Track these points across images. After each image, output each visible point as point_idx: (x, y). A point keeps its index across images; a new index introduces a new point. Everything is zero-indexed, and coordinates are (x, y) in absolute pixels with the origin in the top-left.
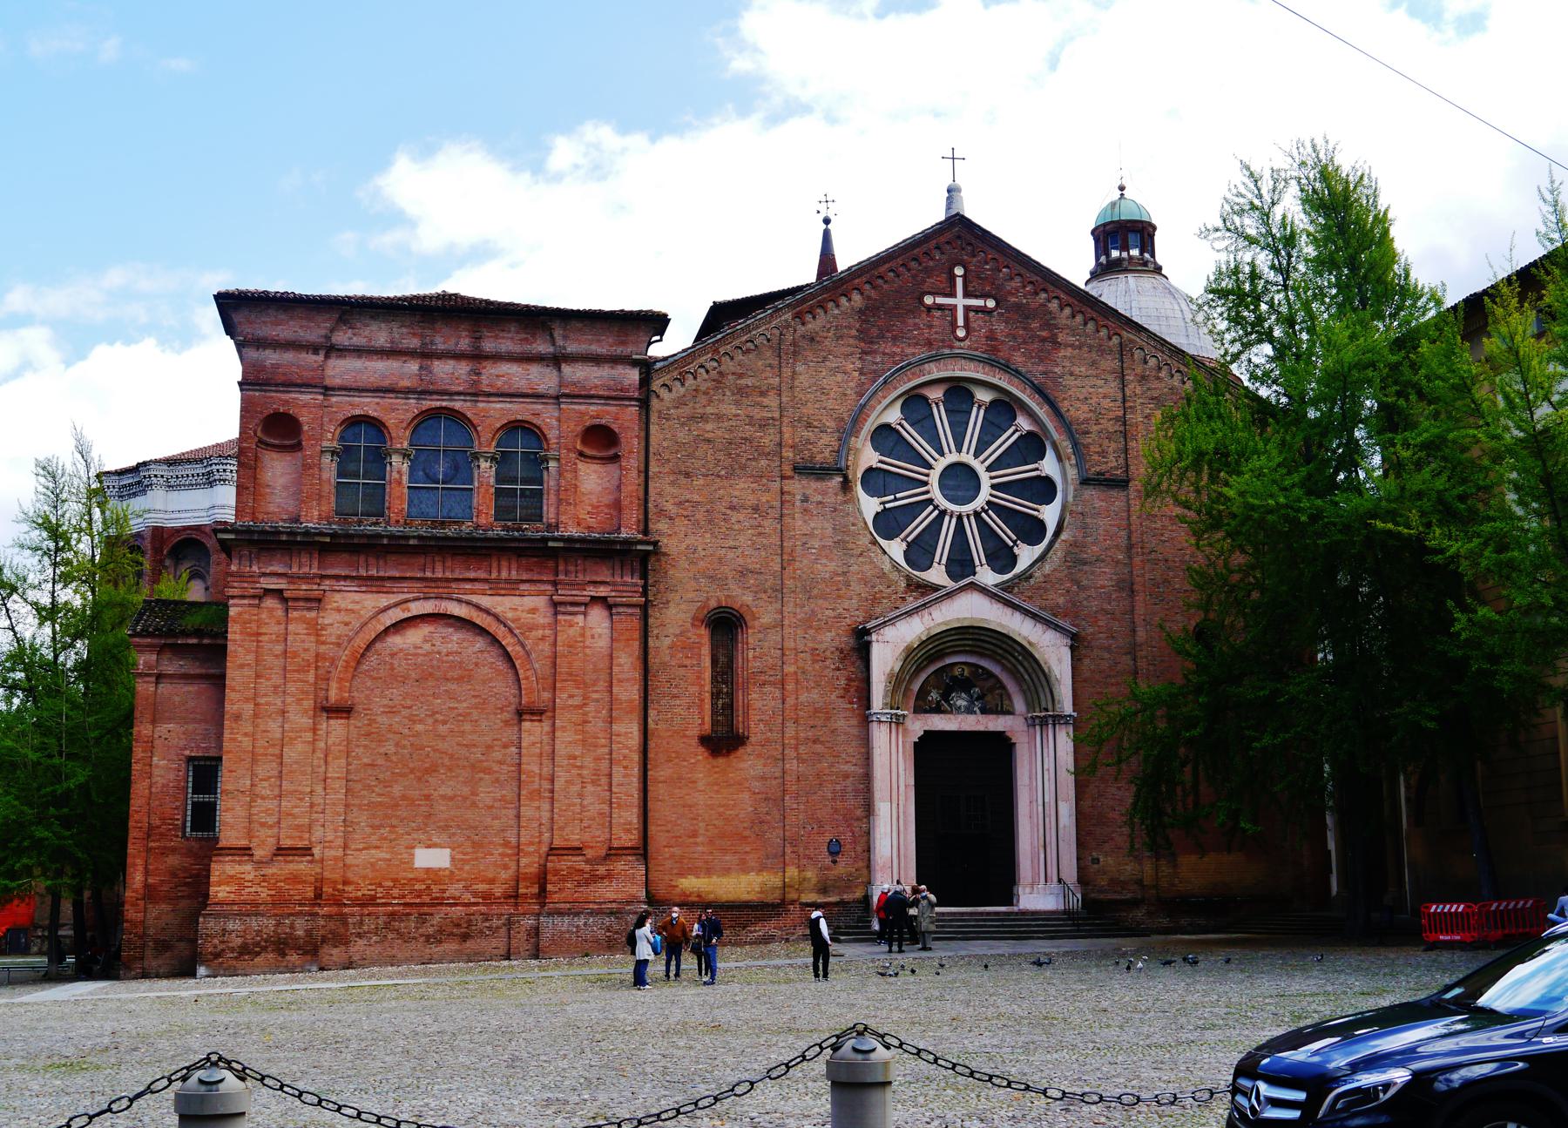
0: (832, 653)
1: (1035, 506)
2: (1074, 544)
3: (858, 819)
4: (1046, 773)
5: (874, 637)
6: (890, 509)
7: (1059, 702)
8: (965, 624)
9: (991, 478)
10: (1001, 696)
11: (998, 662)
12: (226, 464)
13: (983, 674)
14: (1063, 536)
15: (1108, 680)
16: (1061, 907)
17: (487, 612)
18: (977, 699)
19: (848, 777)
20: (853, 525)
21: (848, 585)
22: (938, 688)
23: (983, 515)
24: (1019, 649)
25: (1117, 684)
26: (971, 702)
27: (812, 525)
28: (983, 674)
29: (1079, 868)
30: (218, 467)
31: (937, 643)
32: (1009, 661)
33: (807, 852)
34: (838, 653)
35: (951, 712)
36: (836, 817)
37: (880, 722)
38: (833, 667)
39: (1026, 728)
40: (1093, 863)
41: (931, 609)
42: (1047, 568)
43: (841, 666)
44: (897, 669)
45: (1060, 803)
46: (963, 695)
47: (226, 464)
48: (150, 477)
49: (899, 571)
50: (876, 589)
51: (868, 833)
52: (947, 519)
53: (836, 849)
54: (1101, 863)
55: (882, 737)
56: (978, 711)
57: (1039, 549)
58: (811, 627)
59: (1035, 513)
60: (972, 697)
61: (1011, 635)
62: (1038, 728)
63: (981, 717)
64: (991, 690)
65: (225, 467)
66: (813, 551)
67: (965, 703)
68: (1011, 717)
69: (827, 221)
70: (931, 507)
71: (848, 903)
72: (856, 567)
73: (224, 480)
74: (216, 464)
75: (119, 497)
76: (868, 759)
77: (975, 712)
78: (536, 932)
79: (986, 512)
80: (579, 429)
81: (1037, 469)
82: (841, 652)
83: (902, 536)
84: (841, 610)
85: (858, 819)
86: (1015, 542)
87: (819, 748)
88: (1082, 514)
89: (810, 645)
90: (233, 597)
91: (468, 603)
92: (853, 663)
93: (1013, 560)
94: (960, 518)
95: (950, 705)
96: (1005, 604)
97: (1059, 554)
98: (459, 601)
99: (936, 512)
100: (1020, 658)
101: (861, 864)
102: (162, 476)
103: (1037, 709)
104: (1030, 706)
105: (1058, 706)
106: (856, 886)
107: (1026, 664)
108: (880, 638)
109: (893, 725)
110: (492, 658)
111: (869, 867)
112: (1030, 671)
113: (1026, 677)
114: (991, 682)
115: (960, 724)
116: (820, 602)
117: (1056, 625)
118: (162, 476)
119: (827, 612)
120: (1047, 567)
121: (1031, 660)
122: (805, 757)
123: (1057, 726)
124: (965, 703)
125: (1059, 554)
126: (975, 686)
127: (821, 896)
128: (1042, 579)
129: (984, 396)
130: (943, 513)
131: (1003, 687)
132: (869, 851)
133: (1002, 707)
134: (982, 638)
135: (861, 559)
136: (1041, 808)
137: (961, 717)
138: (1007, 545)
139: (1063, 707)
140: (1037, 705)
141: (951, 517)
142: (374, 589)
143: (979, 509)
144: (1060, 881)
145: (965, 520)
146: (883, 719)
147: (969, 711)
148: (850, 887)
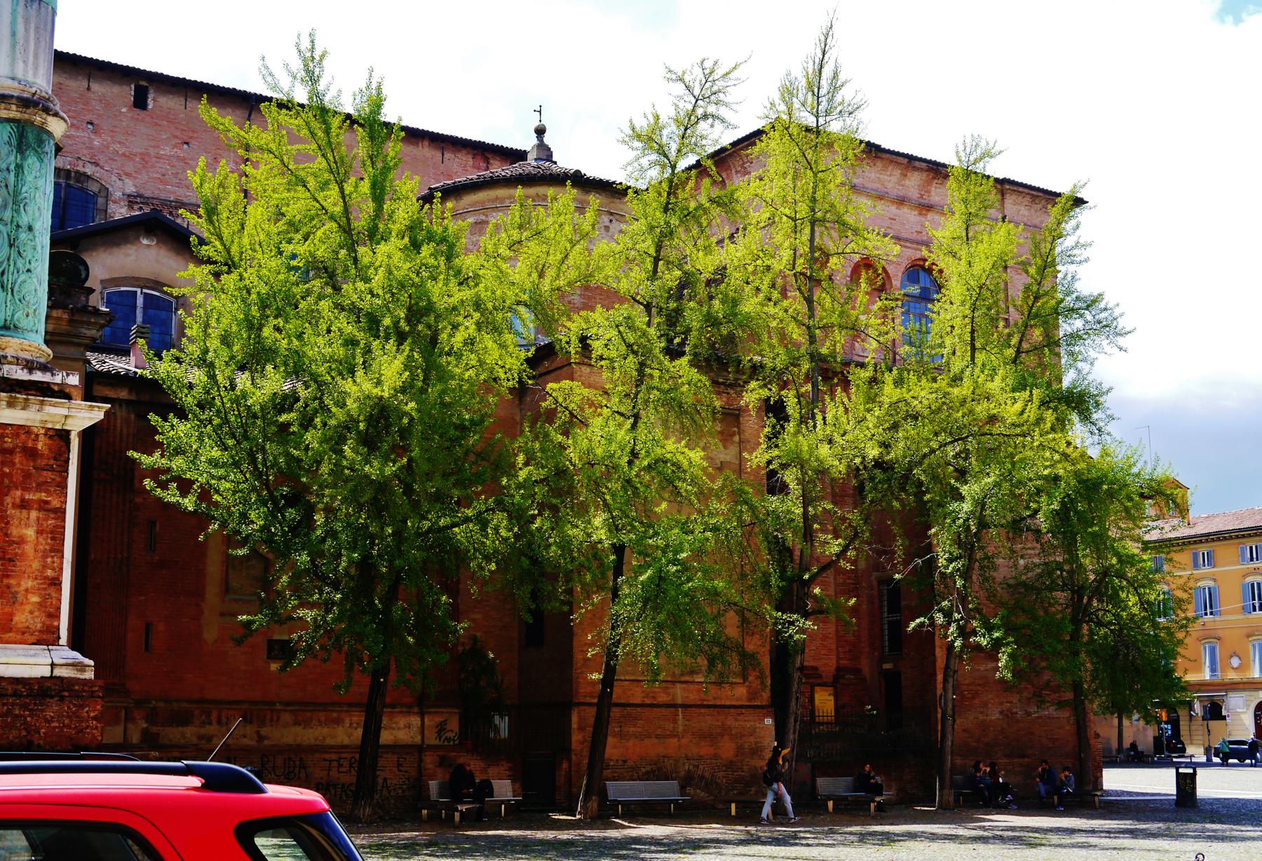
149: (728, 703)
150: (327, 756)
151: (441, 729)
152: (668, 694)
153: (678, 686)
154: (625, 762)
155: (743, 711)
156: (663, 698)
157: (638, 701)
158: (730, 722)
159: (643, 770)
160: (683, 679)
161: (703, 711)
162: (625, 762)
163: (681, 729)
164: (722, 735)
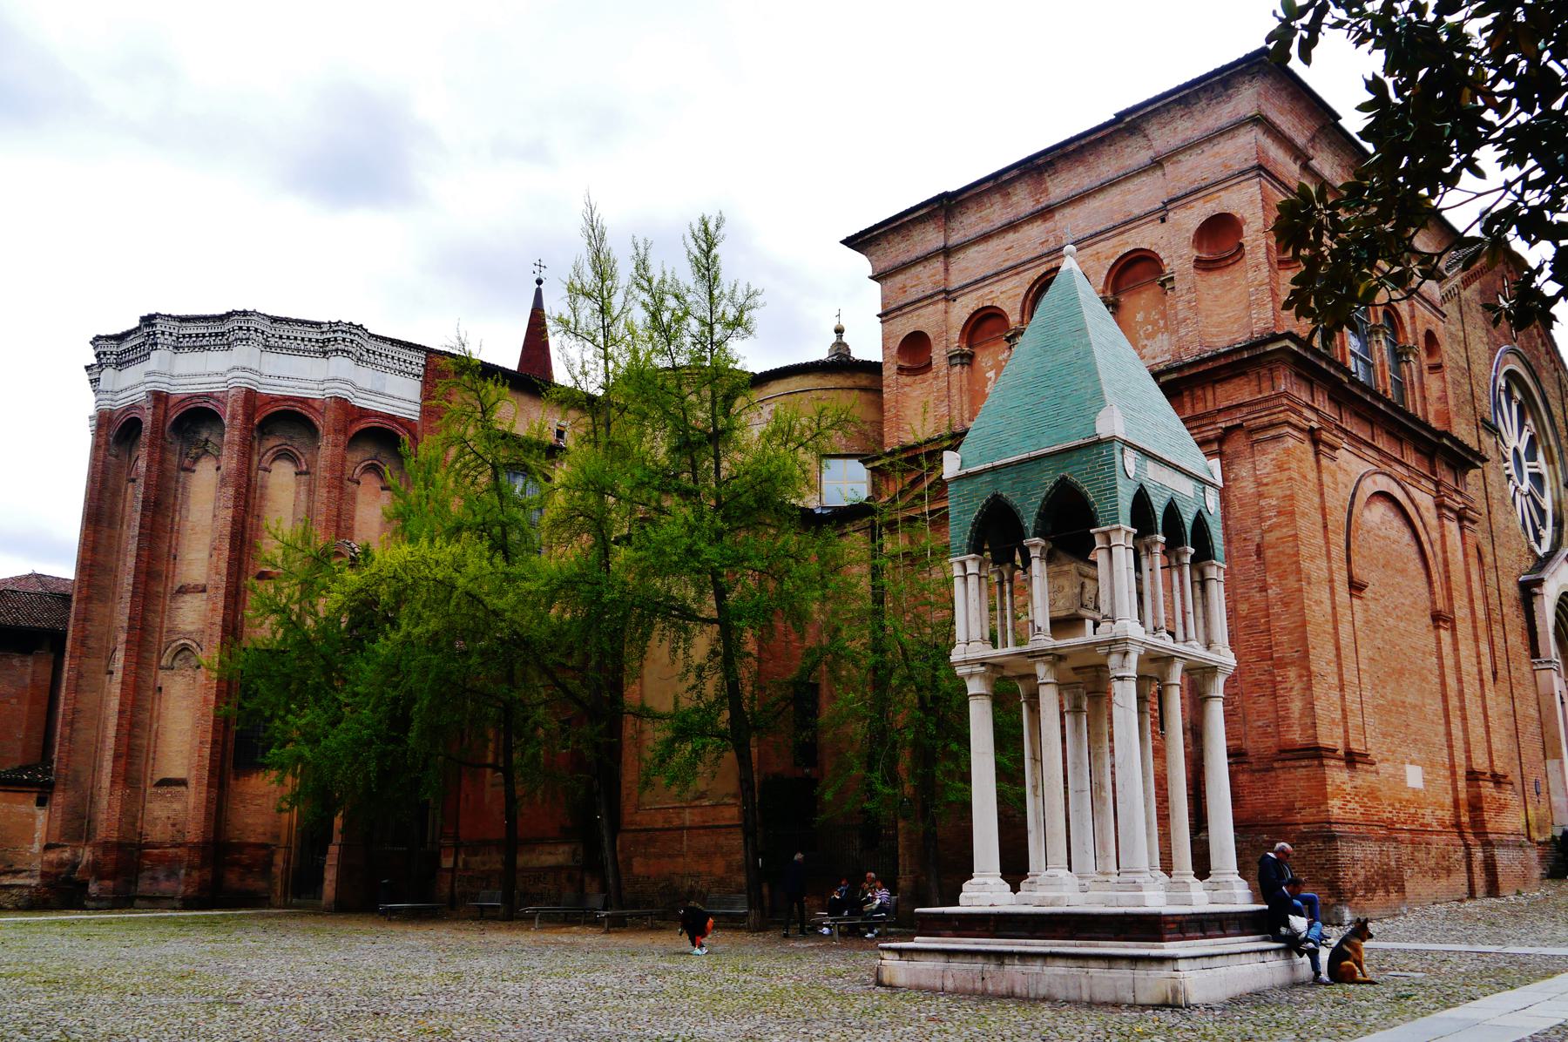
9: (1529, 467)
12: (355, 334)
17: (1412, 501)
30: (344, 335)
47: (355, 334)
48: (248, 329)
65: (352, 337)
69: (539, 282)
73: (348, 352)
74: (343, 332)
75: (176, 348)
78: (1490, 867)
80: (1423, 333)
81: (1536, 467)
90: (1290, 424)
91: (1403, 488)
98: (1399, 484)
102: (263, 333)
110: (1412, 551)
118: (263, 333)
129: (1517, 394)
142: (1356, 451)
149: (723, 823)
150: (525, 874)
151: (574, 853)
152: (679, 818)
153: (688, 810)
154: (649, 878)
155: (732, 830)
156: (676, 822)
157: (659, 825)
158: (722, 841)
159: (661, 885)
160: (693, 804)
161: (701, 832)
162: (649, 878)
163: (685, 850)
164: (715, 853)
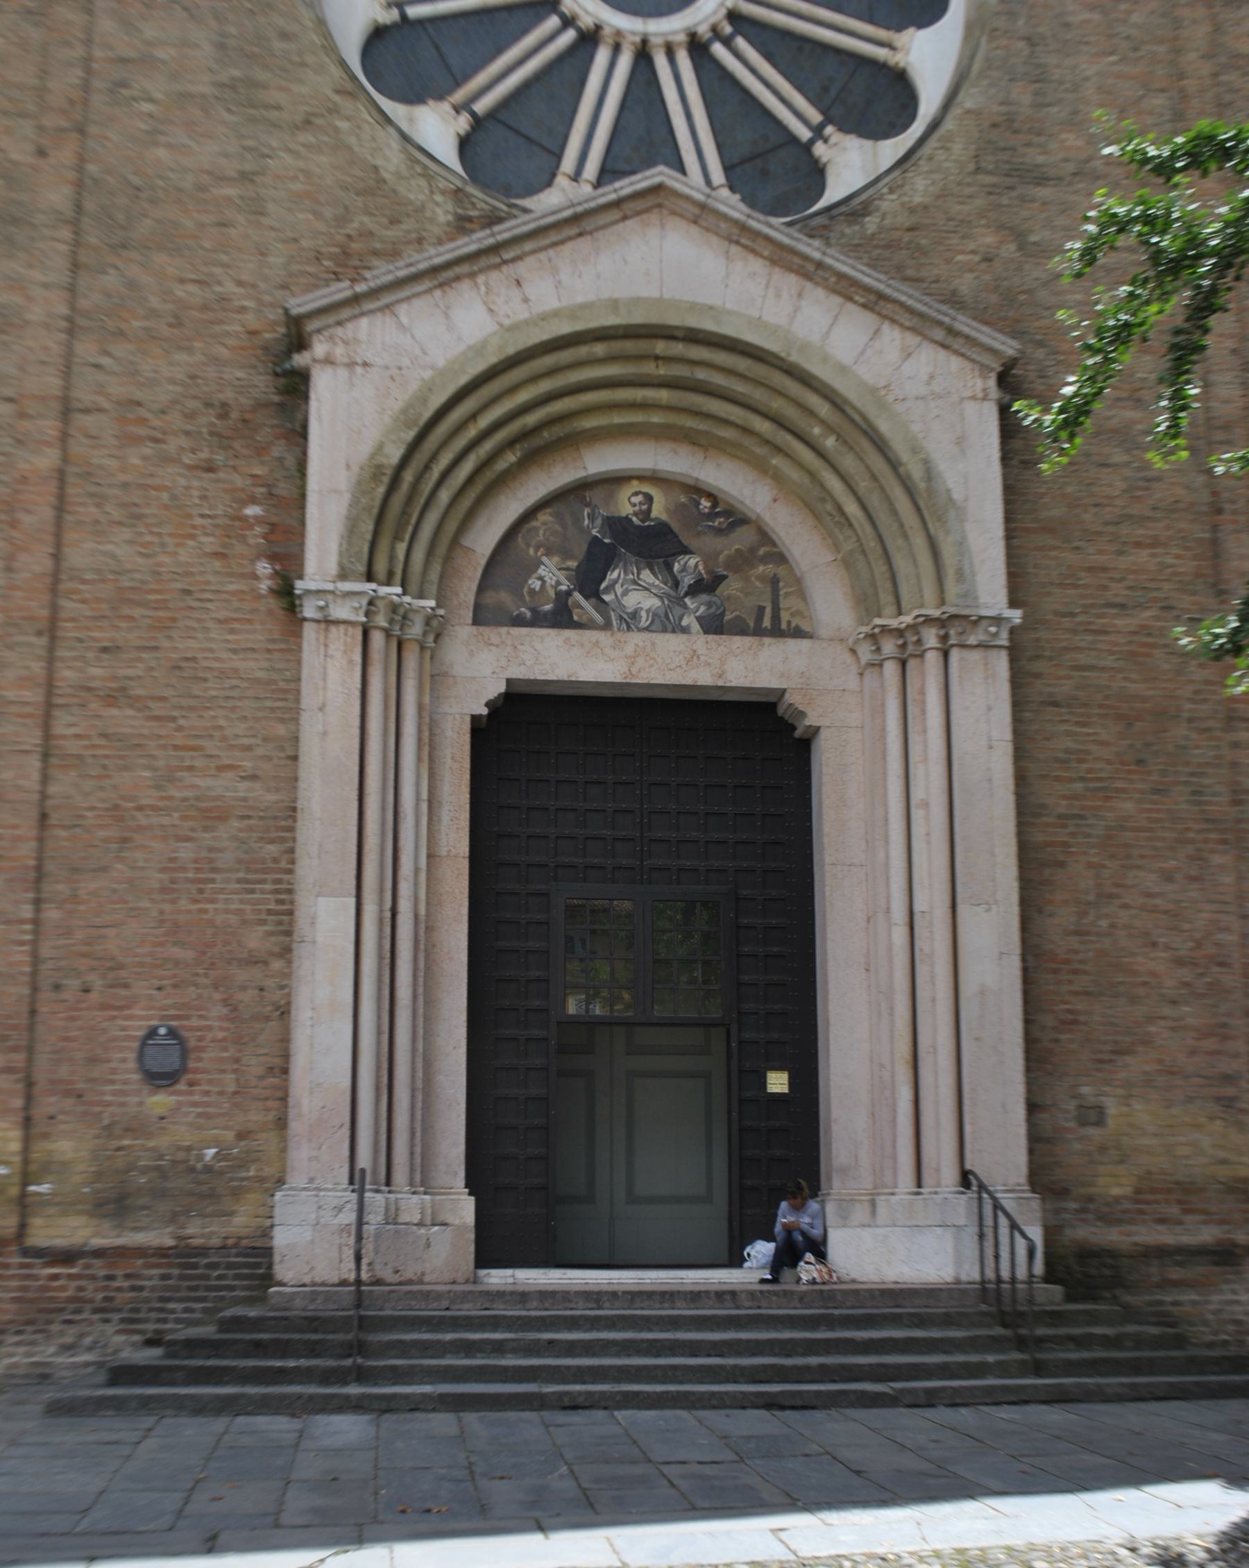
0: (191, 416)
1: (882, 34)
2: (1008, 123)
3: (253, 961)
4: (917, 814)
5: (320, 348)
6: (422, 22)
7: (960, 576)
8: (638, 318)
10: (774, 582)
11: (762, 468)
13: (712, 515)
14: (969, 100)
15: (1125, 530)
16: (971, 1273)
18: (698, 588)
19: (223, 818)
20: (285, 36)
21: (256, 209)
22: (566, 554)
23: (718, 49)
24: (823, 409)
25: (1155, 543)
26: (676, 594)
27: (150, 32)
28: (712, 515)
29: (1036, 1139)
31: (545, 386)
32: (800, 465)
33: (64, 1071)
34: (208, 418)
35: (607, 626)
36: (176, 952)
37: (328, 622)
38: (188, 459)
39: (852, 682)
40: (1083, 1123)
41: (521, 268)
42: (920, 187)
43: (219, 458)
44: (394, 454)
45: (961, 908)
46: (647, 576)
49: (427, 175)
50: (352, 228)
51: (284, 1012)
52: (602, 56)
53: (167, 1060)
54: (1111, 1123)
55: (334, 675)
56: (696, 627)
57: (891, 149)
58: (121, 334)
59: (881, 53)
60: (676, 584)
61: (794, 358)
62: (891, 669)
63: (701, 642)
64: (742, 562)
66: (146, 107)
67: (652, 602)
68: (805, 644)
70: (553, 22)
71: (203, 1251)
72: (288, 159)
76: (295, 758)
77: (685, 630)
79: (727, 42)
82: (224, 416)
83: (460, 95)
84: (230, 288)
85: (253, 961)
86: (818, 131)
87: (125, 719)
88: (1028, 40)
89: (118, 389)
92: (260, 451)
93: (817, 174)
94: (643, 55)
95: (602, 606)
96: (773, 262)
97: (957, 148)
99: (569, 36)
100: (830, 442)
101: (256, 1116)
103: (890, 609)
104: (866, 604)
105: (952, 589)
106: (237, 1194)
107: (848, 462)
108: (339, 351)
109: (377, 639)
111: (281, 1124)
112: (863, 485)
113: (852, 508)
114: (741, 539)
115: (632, 660)
116: (160, 258)
117: (951, 331)
119: (179, 291)
120: (920, 183)
121: (866, 444)
122: (73, 747)
123: (955, 655)
124: (652, 602)
125: (957, 148)
126: (686, 551)
127: (106, 1224)
128: (904, 220)
130: (589, 39)
131: (780, 558)
132: (285, 1071)
133: (776, 618)
134: (701, 374)
135: (306, 137)
136: (899, 935)
137: (636, 639)
138: (793, 139)
139: (969, 595)
140: (886, 598)
141: (617, 49)
143: (703, 30)
144: (966, 1178)
145: (661, 62)
146: (341, 611)
147: (666, 623)
148: (212, 1196)
